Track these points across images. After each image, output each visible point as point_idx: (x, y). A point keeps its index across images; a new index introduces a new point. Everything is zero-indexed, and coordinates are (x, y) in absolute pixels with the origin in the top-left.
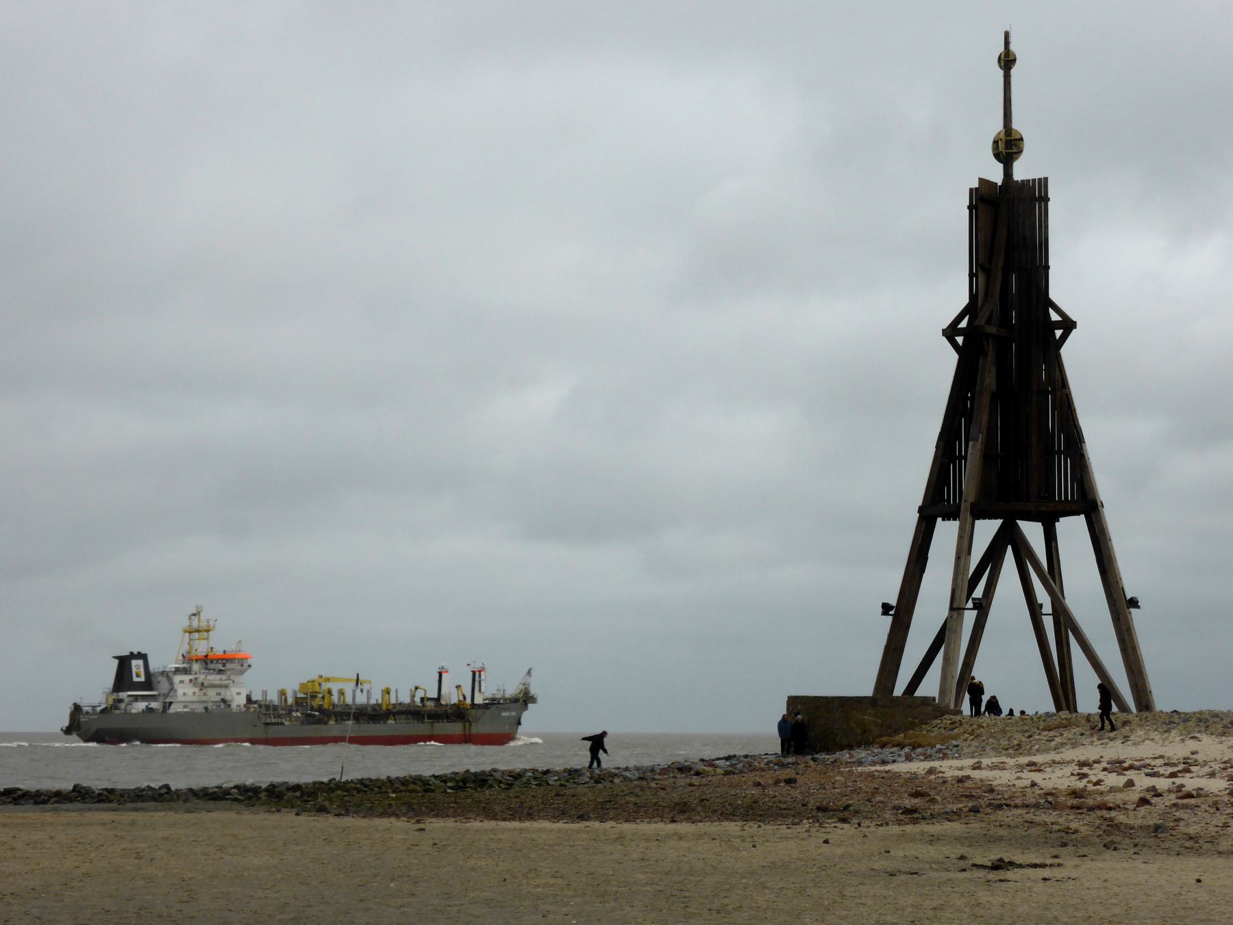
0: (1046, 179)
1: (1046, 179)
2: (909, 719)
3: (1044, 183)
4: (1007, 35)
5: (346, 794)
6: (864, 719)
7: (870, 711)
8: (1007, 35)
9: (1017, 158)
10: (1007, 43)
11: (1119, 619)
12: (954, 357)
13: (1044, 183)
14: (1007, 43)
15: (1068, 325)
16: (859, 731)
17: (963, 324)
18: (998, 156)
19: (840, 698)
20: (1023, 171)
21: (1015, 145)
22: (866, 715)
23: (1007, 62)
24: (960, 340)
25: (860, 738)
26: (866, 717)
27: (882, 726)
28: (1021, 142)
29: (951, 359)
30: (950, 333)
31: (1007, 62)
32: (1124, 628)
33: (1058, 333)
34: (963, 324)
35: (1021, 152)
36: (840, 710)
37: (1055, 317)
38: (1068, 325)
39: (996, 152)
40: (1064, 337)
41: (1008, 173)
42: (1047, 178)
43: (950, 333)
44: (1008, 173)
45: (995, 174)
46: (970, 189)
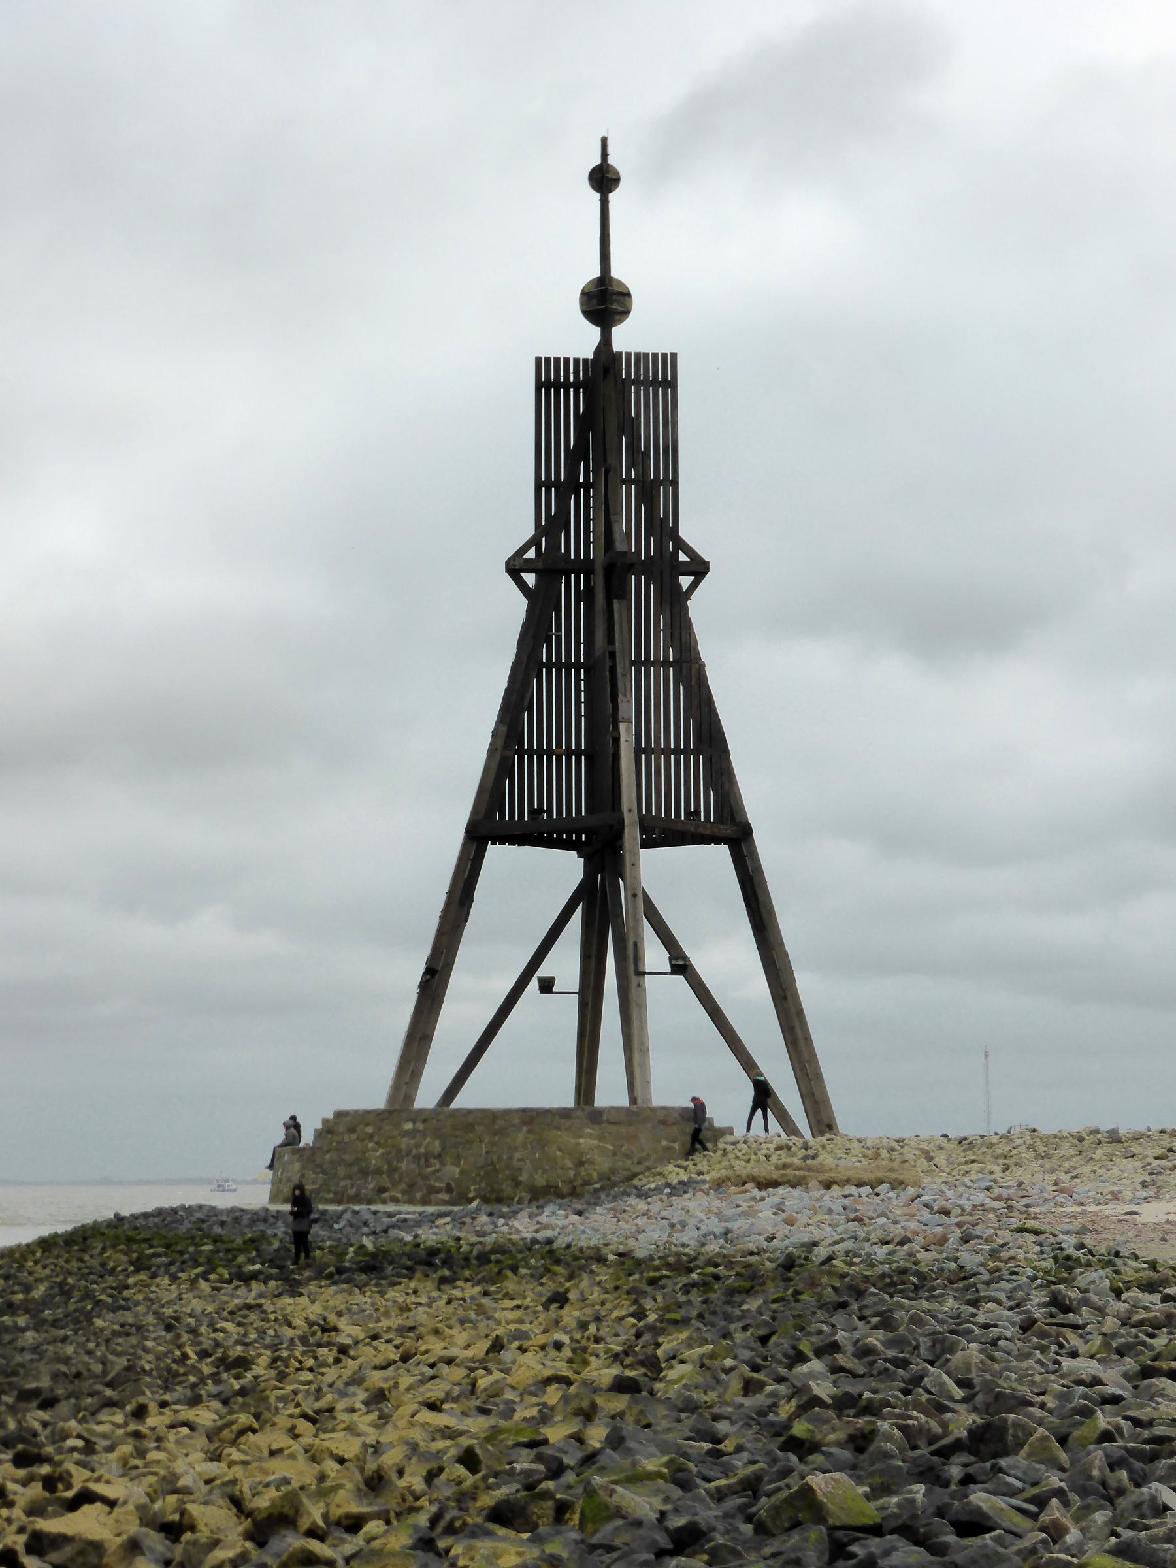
0: (674, 356)
1: (674, 356)
2: (664, 1143)
3: (670, 361)
4: (604, 142)
5: (274, 1271)
6: (579, 1144)
7: (588, 1130)
8: (604, 142)
9: (621, 321)
10: (605, 154)
11: (785, 998)
12: (520, 604)
13: (670, 361)
14: (605, 154)
15: (699, 569)
16: (568, 1163)
19: (524, 1110)
20: (625, 339)
21: (616, 301)
22: (581, 1137)
24: (530, 579)
25: (572, 1173)
26: (581, 1140)
27: (614, 1154)
28: (627, 298)
29: (517, 607)
30: (515, 568)
32: (793, 1010)
35: (626, 312)
36: (524, 1129)
37: (683, 557)
39: (585, 308)
40: (694, 586)
42: (676, 354)
43: (515, 568)
44: (606, 340)
46: (538, 360)
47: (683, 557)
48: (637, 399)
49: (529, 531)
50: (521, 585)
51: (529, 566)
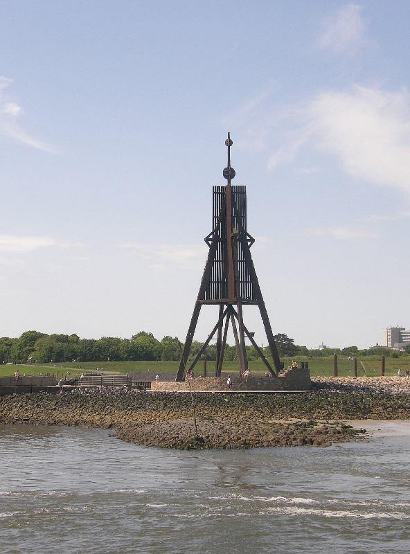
10: (229, 137)
14: (229, 137)
15: (252, 240)
17: (211, 237)
18: (225, 176)
20: (234, 182)
23: (229, 143)
24: (210, 242)
30: (207, 240)
31: (229, 143)
33: (249, 243)
34: (211, 237)
38: (252, 240)
41: (229, 182)
43: (207, 240)
44: (229, 182)
45: (223, 183)
47: (248, 238)
48: (238, 199)
49: (211, 231)
50: (208, 244)
51: (210, 240)
